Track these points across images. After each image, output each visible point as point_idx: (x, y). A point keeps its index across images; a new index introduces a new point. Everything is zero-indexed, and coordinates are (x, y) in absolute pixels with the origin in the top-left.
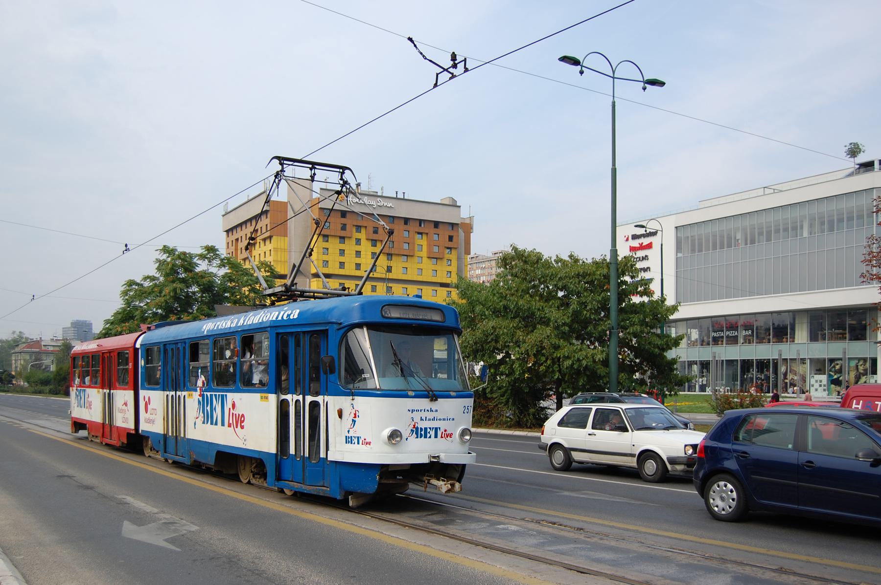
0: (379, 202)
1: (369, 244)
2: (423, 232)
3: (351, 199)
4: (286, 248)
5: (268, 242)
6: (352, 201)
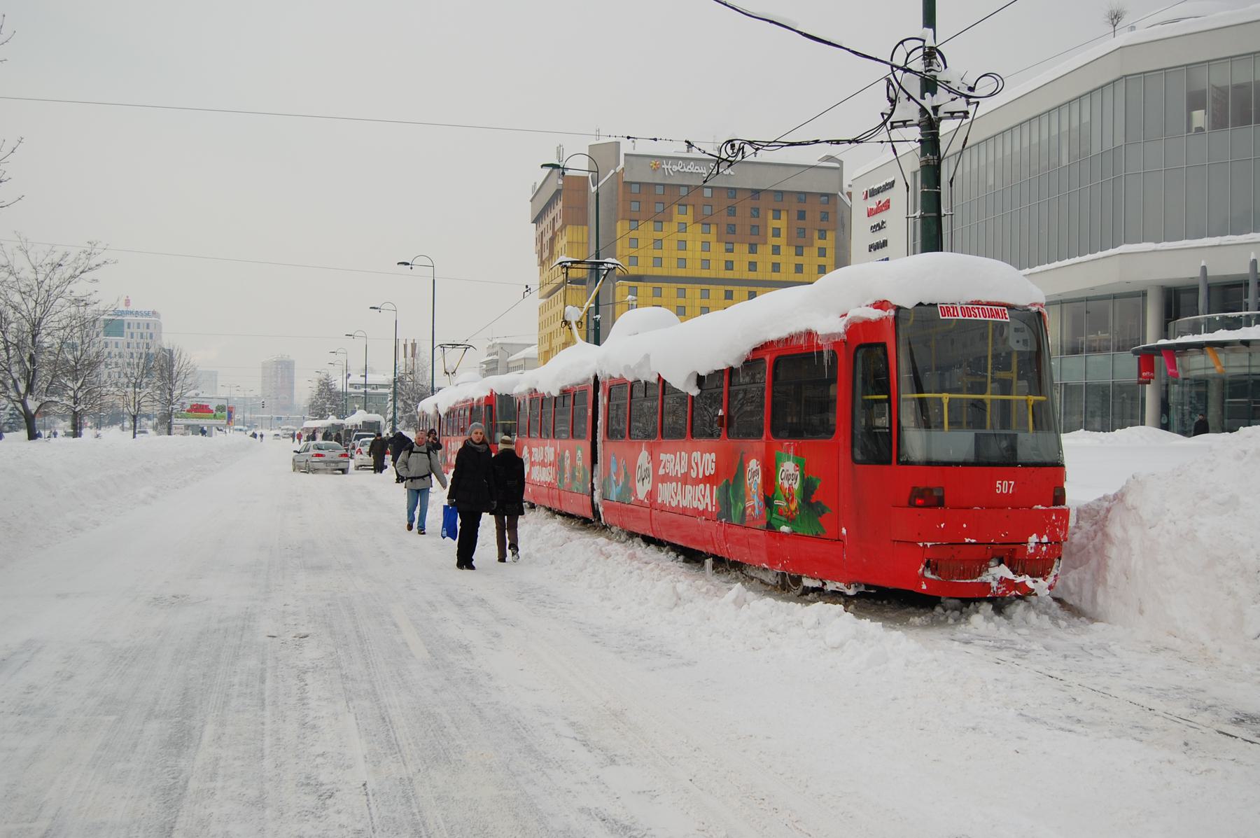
1: (699, 227)
3: (669, 167)
4: (585, 241)
6: (671, 169)
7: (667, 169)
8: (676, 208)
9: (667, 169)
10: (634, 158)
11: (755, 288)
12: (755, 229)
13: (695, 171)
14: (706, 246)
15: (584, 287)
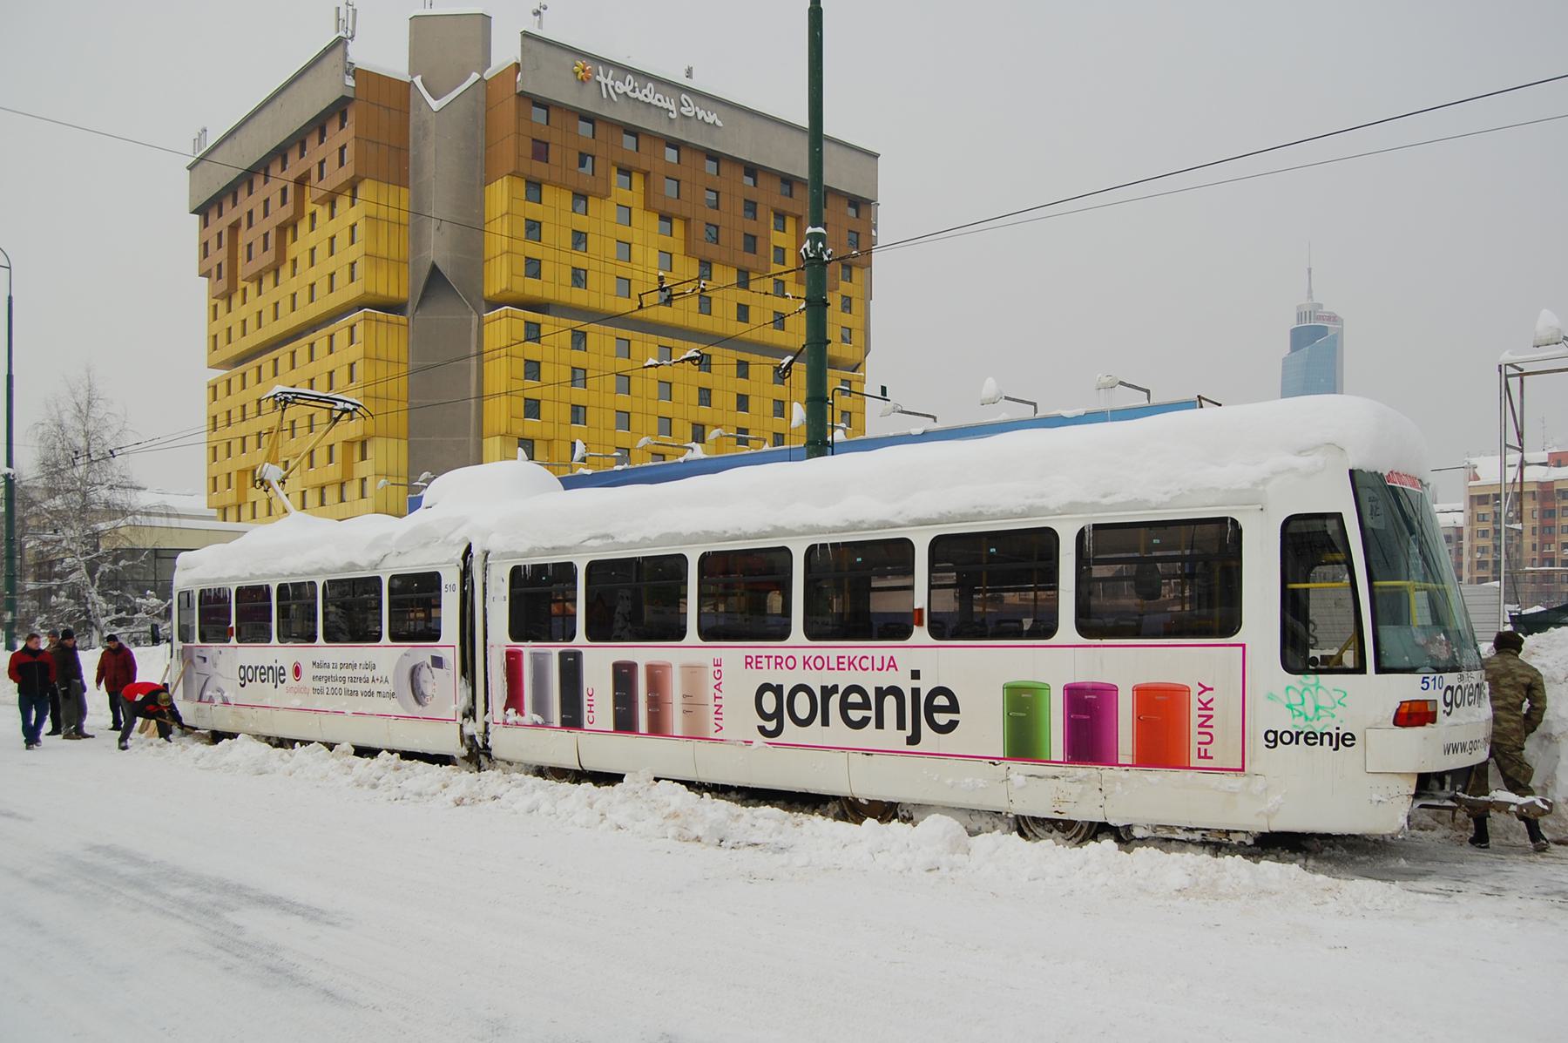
0: (683, 106)
2: (789, 209)
3: (611, 84)
5: (343, 202)
6: (613, 87)
7: (606, 85)
8: (615, 177)
9: (606, 85)
10: (541, 47)
11: (747, 354)
12: (751, 243)
13: (655, 102)
14: (667, 257)
15: (402, 319)
